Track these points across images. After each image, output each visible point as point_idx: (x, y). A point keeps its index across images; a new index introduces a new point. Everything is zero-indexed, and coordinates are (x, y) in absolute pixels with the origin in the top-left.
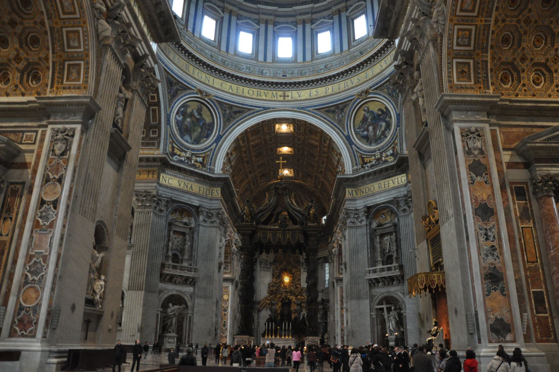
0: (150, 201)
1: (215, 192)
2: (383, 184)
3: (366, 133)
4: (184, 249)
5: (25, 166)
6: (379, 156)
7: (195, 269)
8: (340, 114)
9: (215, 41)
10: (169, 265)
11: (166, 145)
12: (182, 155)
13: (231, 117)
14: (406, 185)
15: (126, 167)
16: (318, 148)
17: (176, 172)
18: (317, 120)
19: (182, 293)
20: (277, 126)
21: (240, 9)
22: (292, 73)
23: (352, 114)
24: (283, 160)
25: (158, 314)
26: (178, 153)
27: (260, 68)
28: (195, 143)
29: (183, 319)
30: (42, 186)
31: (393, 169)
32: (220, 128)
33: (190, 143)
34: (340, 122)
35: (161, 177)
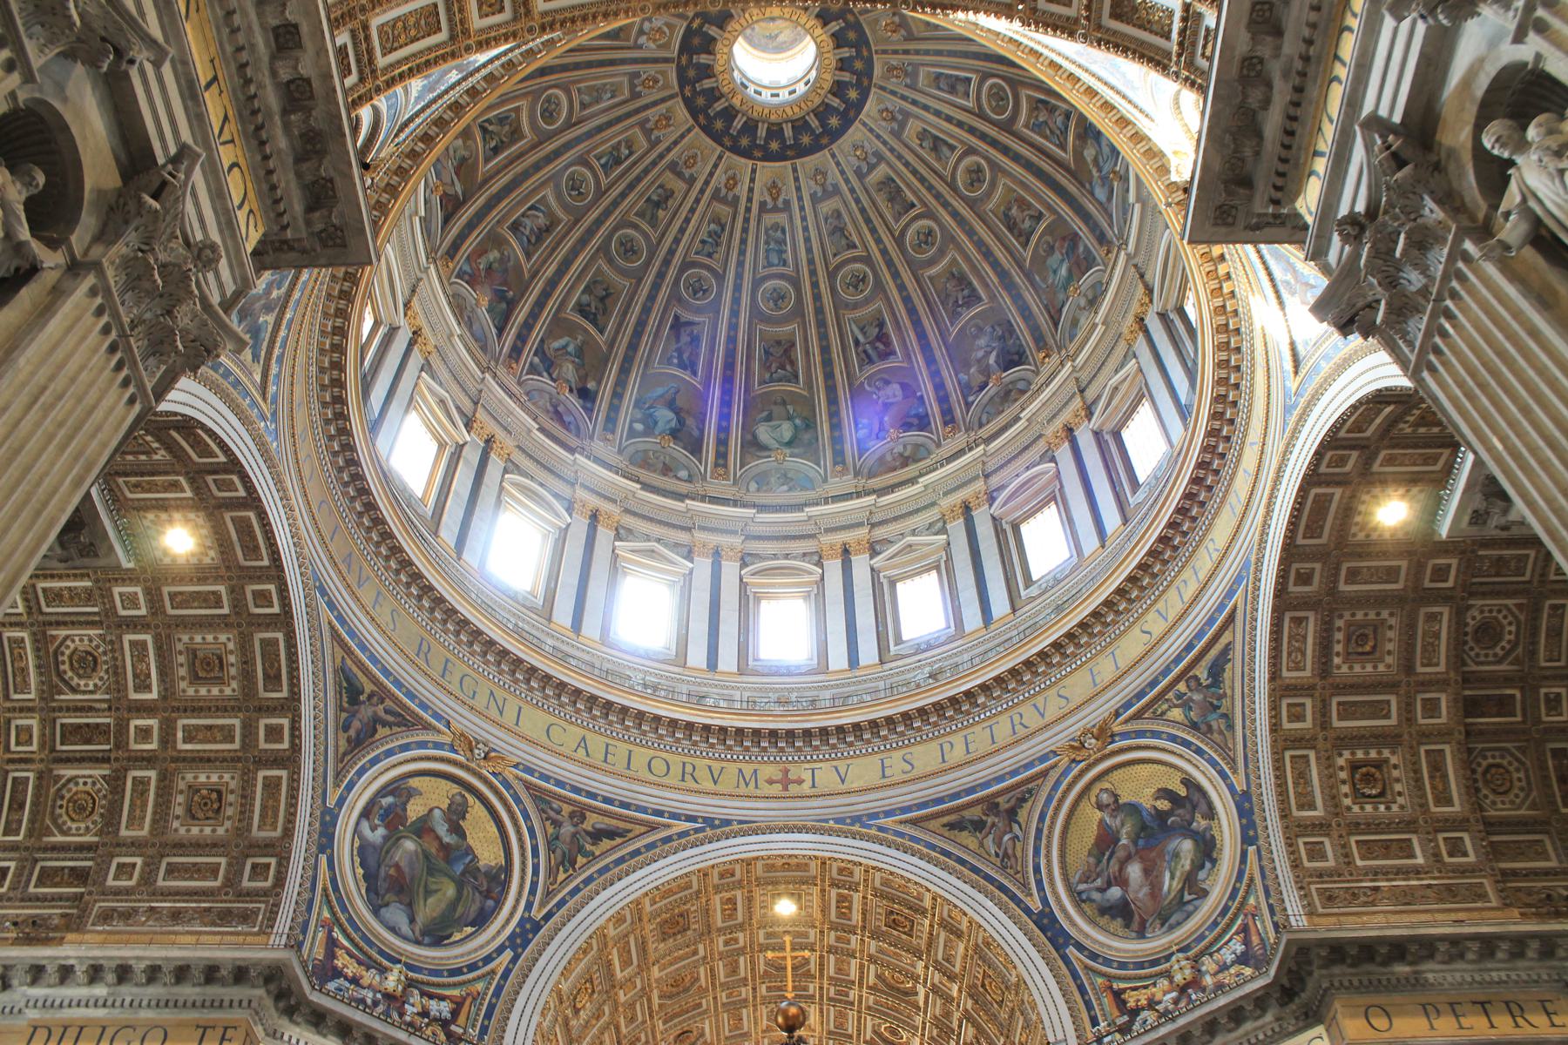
3: (1115, 892)
6: (1188, 972)
8: (1005, 833)
11: (304, 931)
12: (365, 981)
13: (581, 850)
16: (921, 991)
18: (915, 860)
21: (627, 511)
23: (1051, 827)
26: (352, 969)
27: (693, 688)
28: (427, 940)
31: (1264, 1010)
32: (533, 892)
33: (405, 938)
34: (1006, 859)
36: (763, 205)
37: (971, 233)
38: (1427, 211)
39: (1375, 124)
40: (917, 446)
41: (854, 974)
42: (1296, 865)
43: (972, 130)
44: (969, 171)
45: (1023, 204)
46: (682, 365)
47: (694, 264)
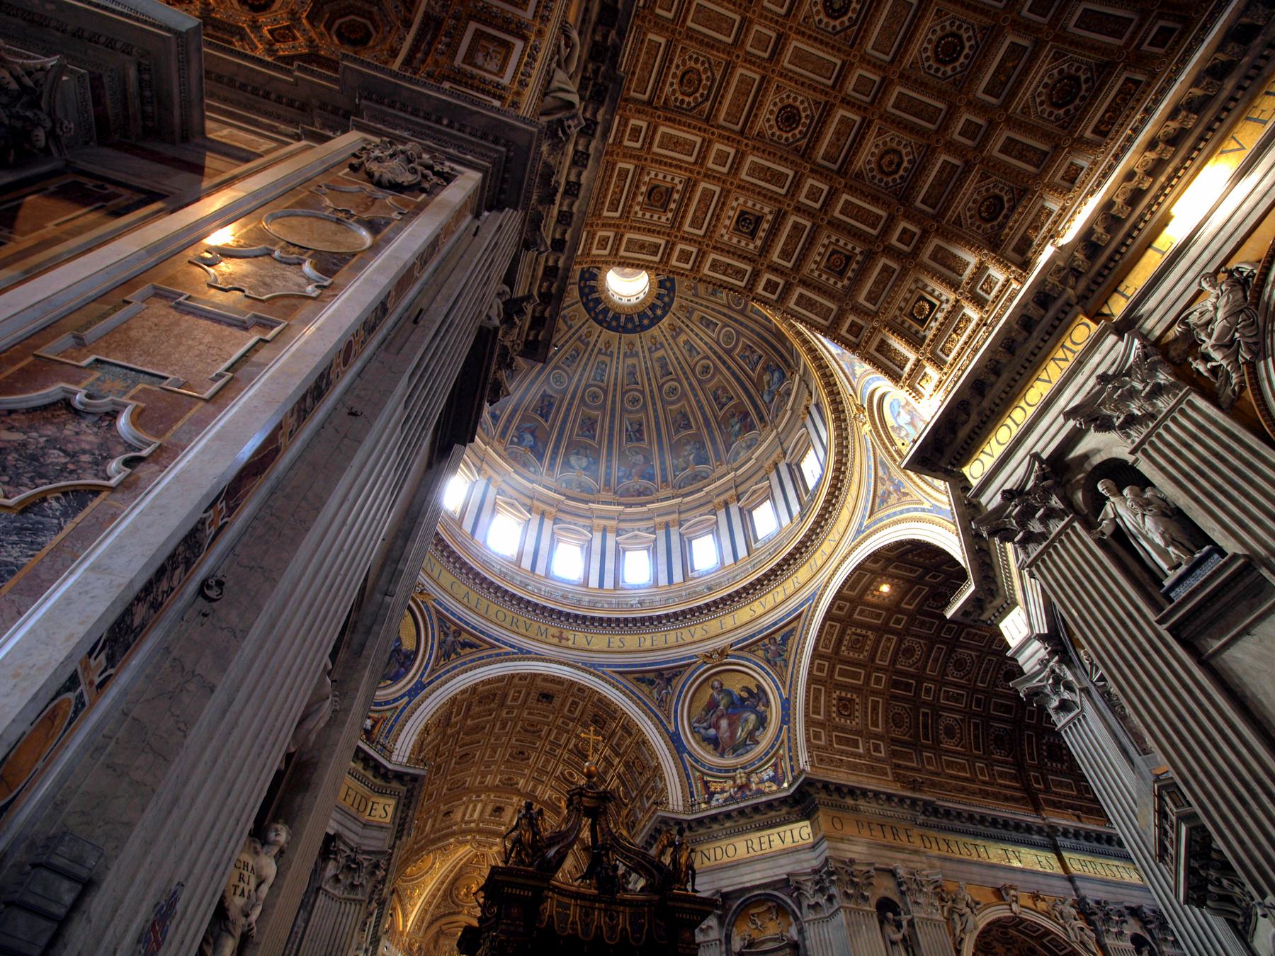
2: (756, 842)
3: (712, 731)
13: (455, 650)
14: (813, 847)
32: (425, 669)
34: (661, 702)
36: (600, 350)
37: (696, 395)
38: (1053, 502)
39: (1036, 457)
40: (646, 488)
41: (563, 741)
42: (808, 740)
43: (711, 348)
44: (703, 367)
45: (724, 389)
46: (541, 415)
47: (559, 368)
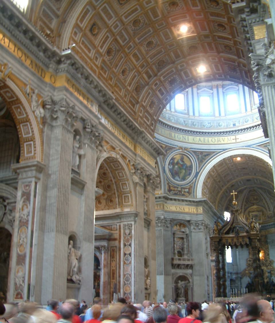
0: (161, 222)
1: (198, 209)
4: (184, 247)
5: (115, 239)
7: (192, 259)
9: (185, 110)
10: (176, 258)
13: (203, 159)
15: (151, 228)
17: (174, 202)
19: (186, 274)
20: (234, 159)
22: (239, 121)
24: (235, 192)
25: (173, 288)
28: (182, 180)
29: (188, 289)
30: (124, 248)
35: (165, 207)
